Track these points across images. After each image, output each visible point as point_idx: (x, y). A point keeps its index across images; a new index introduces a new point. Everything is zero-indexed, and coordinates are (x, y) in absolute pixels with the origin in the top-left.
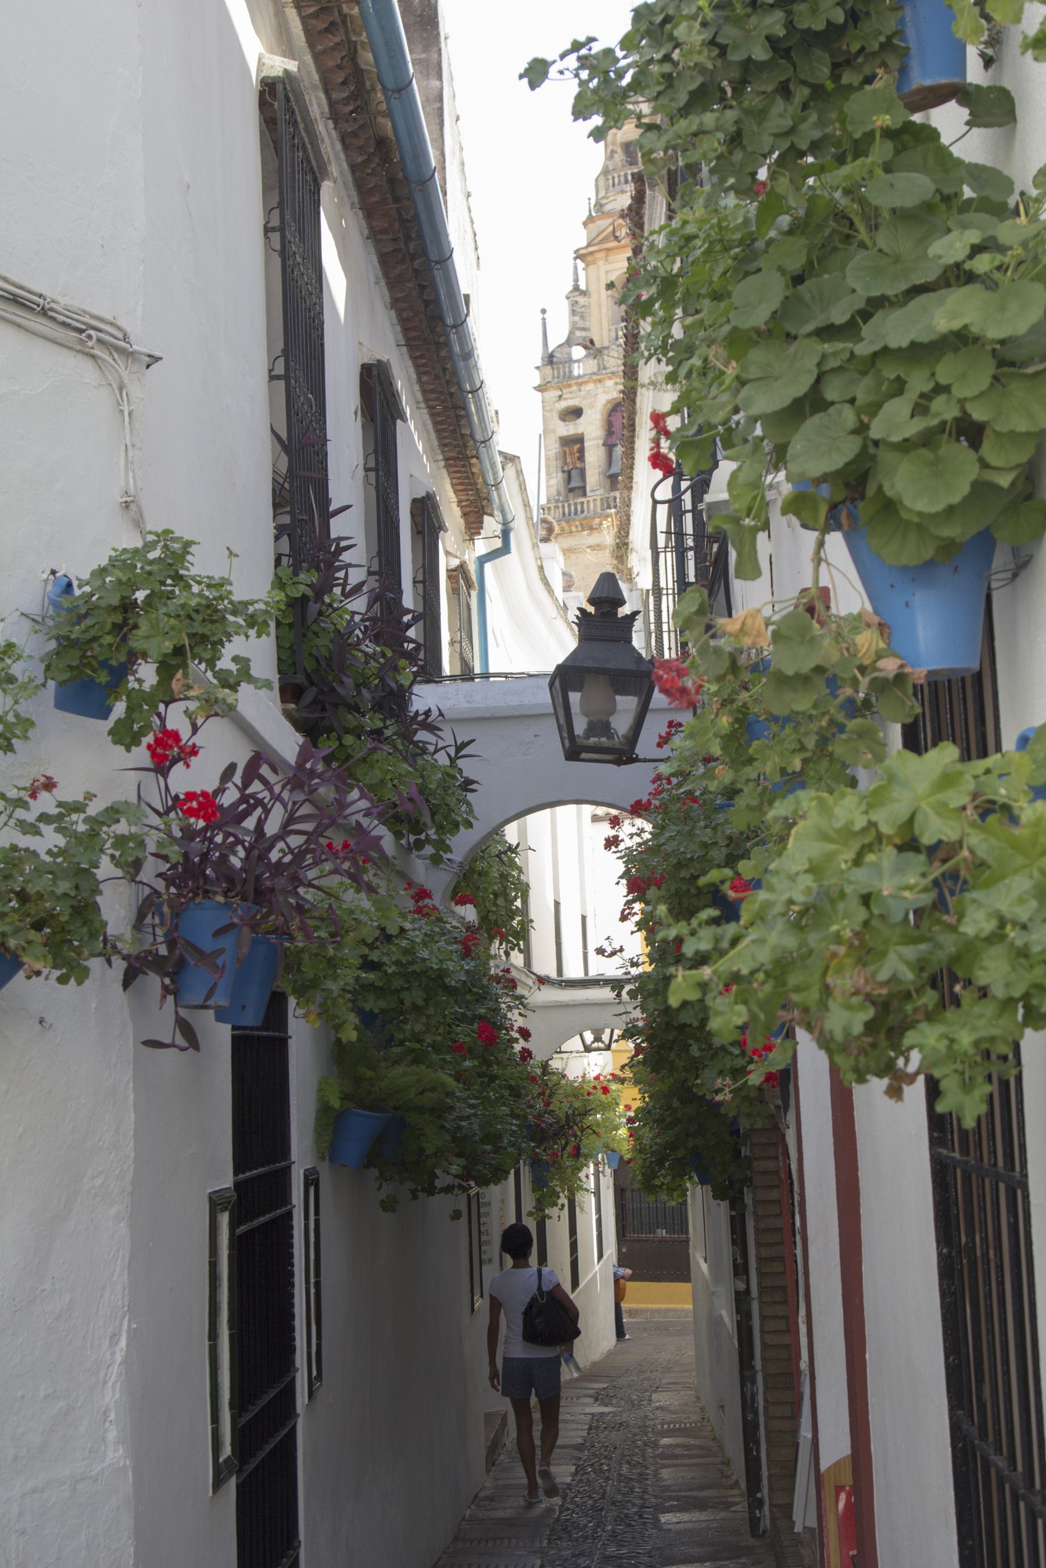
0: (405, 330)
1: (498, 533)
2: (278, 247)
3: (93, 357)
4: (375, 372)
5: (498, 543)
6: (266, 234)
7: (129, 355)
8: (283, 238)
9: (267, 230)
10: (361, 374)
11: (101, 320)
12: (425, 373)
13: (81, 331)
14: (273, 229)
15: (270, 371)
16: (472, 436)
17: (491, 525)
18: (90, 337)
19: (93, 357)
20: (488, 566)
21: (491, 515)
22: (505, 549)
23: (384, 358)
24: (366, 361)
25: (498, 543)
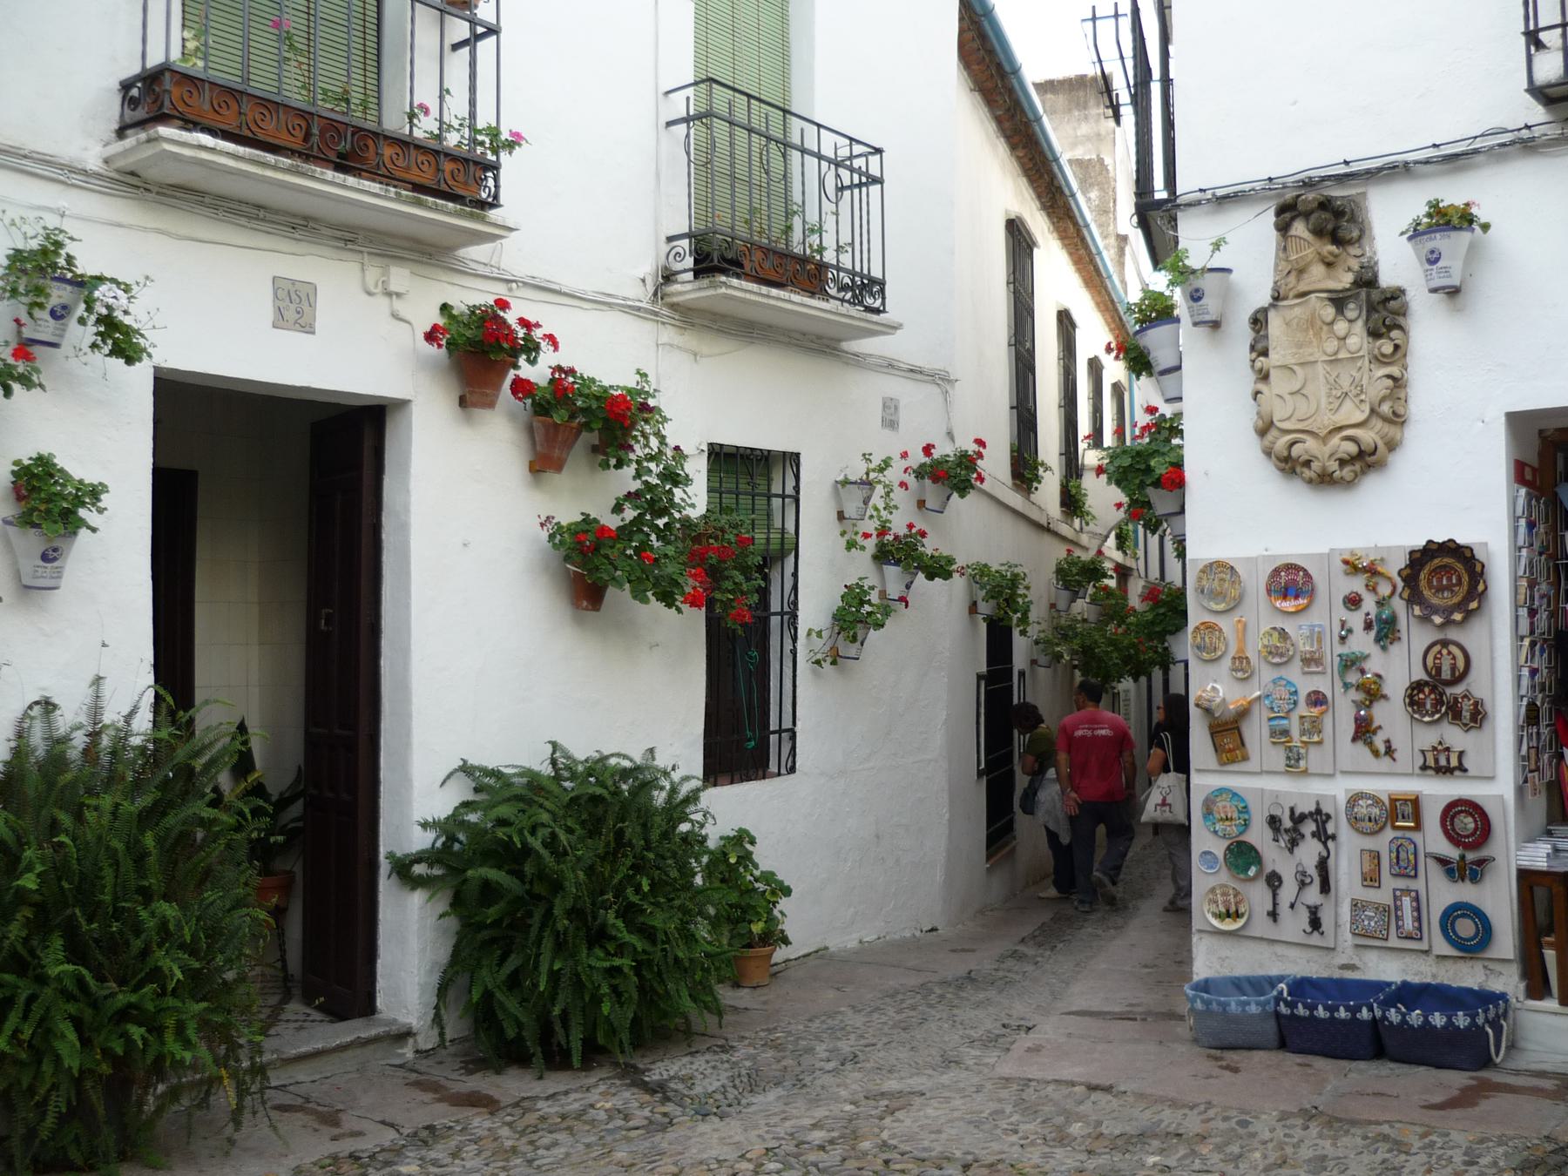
7: (949, 381)
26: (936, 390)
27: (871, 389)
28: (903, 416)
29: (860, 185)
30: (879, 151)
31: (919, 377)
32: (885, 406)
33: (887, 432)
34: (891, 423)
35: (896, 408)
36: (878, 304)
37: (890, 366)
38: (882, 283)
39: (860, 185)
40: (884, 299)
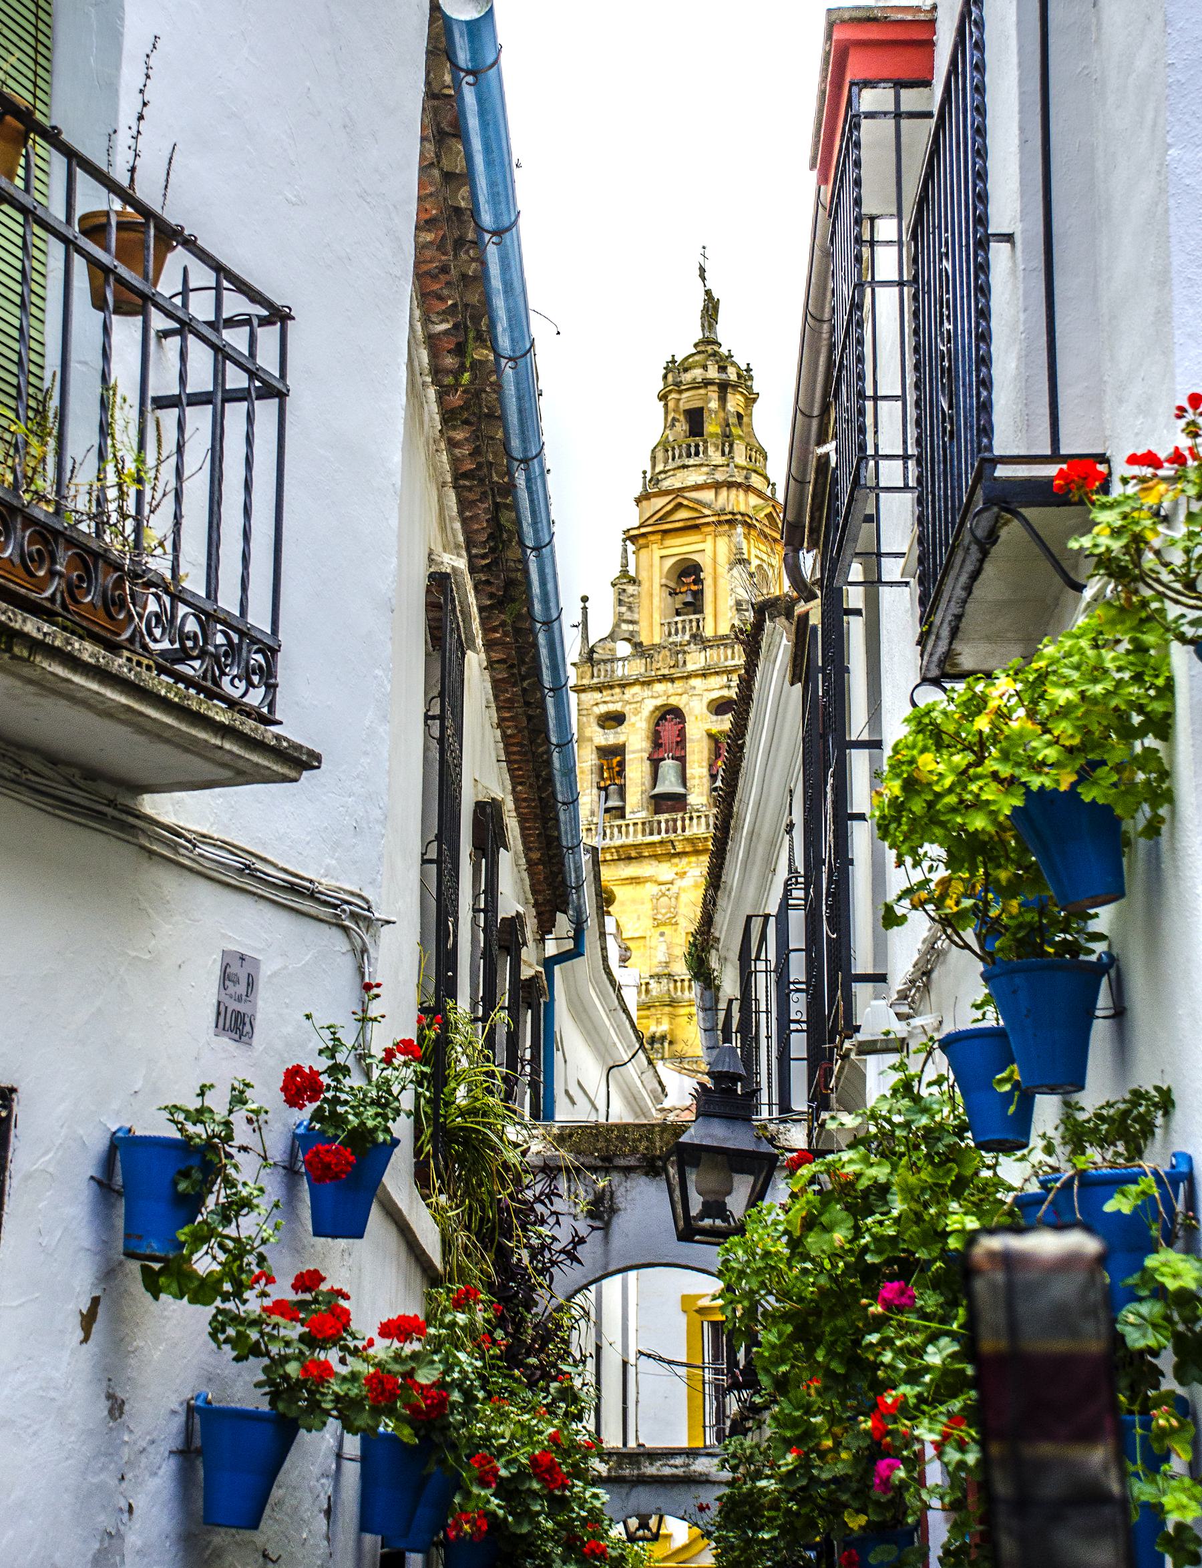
0: (507, 746)
1: (571, 934)
2: (437, 735)
3: (345, 929)
4: (489, 810)
5: (570, 945)
6: (426, 724)
7: (369, 922)
8: (443, 729)
9: (427, 717)
10: (475, 812)
11: (352, 894)
12: (521, 784)
13: (335, 907)
14: (433, 718)
15: (423, 854)
16: (558, 839)
17: (563, 923)
18: (344, 911)
19: (345, 929)
20: (557, 968)
21: (565, 912)
22: (577, 952)
23: (499, 796)
24: (480, 798)
25: (570, 945)
26: (339, 942)
27: (204, 927)
28: (267, 1009)
29: (218, 398)
30: (279, 316)
31: (306, 905)
32: (226, 977)
33: (225, 1042)
34: (235, 1024)
35: (251, 983)
36: (255, 697)
37: (247, 877)
38: (271, 652)
39: (218, 398)
40: (271, 688)
